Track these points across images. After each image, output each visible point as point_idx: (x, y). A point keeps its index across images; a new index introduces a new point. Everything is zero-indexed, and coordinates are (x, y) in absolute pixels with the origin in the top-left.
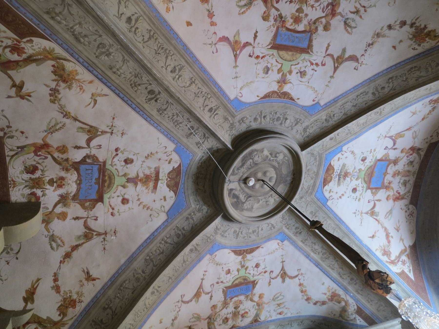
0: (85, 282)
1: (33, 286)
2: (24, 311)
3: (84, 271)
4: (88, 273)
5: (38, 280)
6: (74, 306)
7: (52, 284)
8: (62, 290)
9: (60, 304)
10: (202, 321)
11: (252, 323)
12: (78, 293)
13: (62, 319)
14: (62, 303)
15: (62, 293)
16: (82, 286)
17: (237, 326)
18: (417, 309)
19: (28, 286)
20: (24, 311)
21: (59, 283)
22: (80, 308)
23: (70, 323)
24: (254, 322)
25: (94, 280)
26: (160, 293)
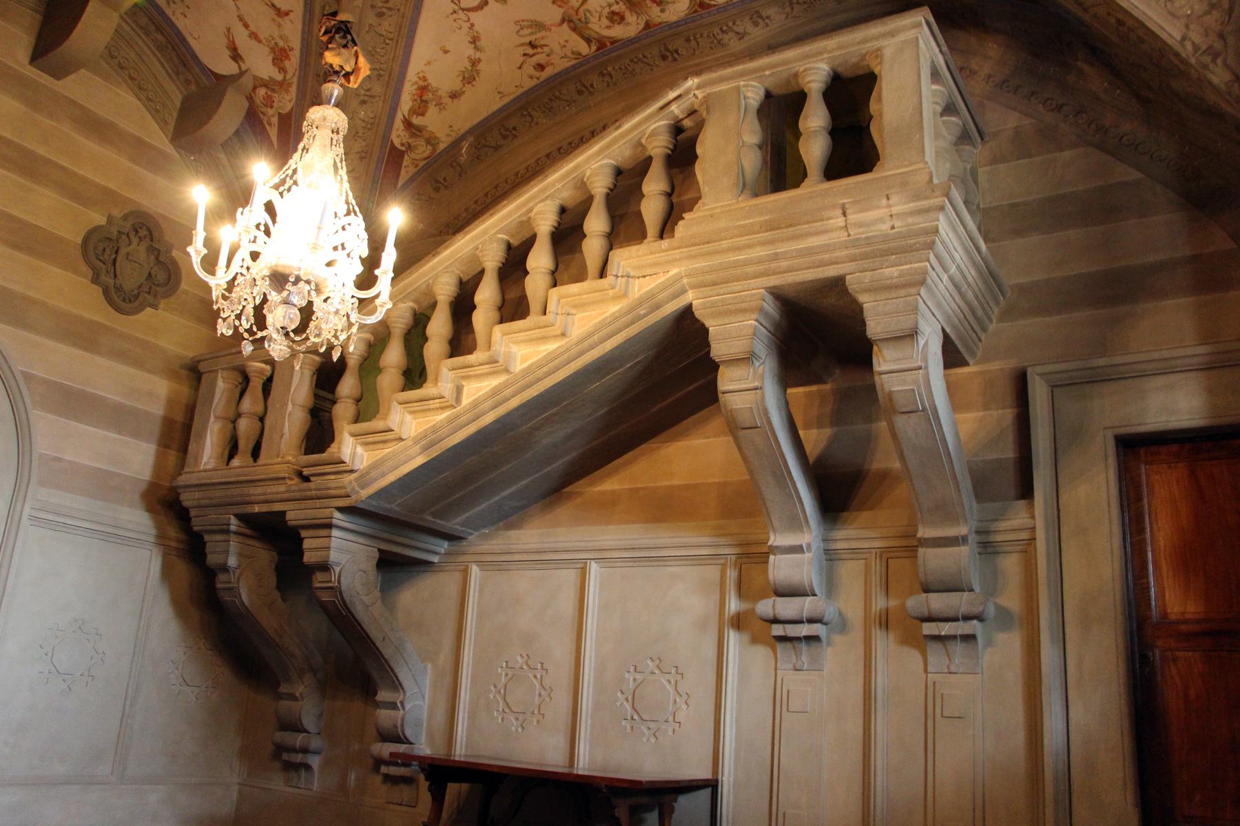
0: (280, 20)
1: (229, 40)
2: (242, 73)
3: (267, 4)
4: (273, 6)
5: (229, 30)
6: (288, 57)
7: (246, 33)
8: (262, 37)
9: (270, 58)
10: (553, 29)
11: (696, 11)
12: (281, 37)
13: (285, 77)
14: (272, 55)
15: (264, 41)
16: (279, 25)
17: (660, 23)
18: (323, 136)
19: (225, 41)
20: (242, 73)
21: (252, 28)
22: (295, 57)
23: (295, 80)
24: (698, 9)
25: (287, 14)
26: (399, 10)
